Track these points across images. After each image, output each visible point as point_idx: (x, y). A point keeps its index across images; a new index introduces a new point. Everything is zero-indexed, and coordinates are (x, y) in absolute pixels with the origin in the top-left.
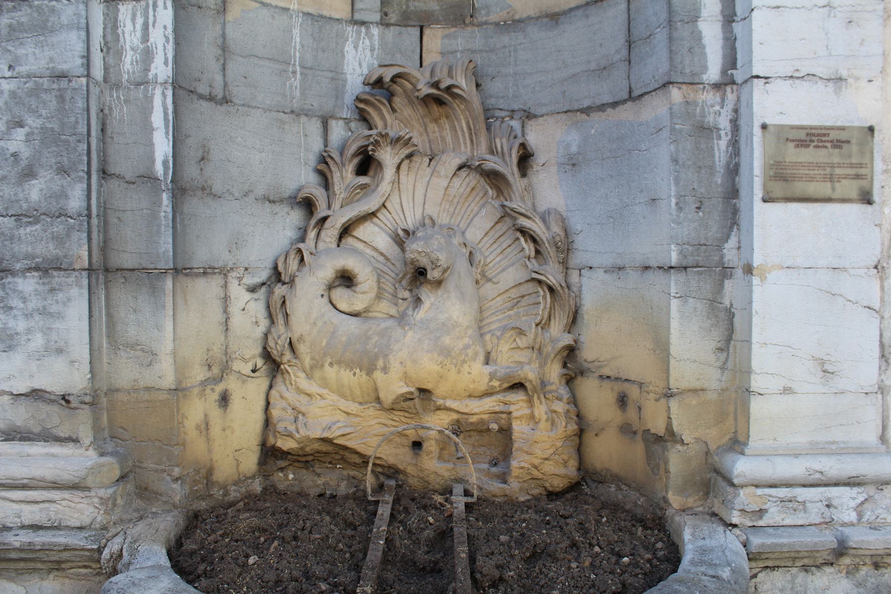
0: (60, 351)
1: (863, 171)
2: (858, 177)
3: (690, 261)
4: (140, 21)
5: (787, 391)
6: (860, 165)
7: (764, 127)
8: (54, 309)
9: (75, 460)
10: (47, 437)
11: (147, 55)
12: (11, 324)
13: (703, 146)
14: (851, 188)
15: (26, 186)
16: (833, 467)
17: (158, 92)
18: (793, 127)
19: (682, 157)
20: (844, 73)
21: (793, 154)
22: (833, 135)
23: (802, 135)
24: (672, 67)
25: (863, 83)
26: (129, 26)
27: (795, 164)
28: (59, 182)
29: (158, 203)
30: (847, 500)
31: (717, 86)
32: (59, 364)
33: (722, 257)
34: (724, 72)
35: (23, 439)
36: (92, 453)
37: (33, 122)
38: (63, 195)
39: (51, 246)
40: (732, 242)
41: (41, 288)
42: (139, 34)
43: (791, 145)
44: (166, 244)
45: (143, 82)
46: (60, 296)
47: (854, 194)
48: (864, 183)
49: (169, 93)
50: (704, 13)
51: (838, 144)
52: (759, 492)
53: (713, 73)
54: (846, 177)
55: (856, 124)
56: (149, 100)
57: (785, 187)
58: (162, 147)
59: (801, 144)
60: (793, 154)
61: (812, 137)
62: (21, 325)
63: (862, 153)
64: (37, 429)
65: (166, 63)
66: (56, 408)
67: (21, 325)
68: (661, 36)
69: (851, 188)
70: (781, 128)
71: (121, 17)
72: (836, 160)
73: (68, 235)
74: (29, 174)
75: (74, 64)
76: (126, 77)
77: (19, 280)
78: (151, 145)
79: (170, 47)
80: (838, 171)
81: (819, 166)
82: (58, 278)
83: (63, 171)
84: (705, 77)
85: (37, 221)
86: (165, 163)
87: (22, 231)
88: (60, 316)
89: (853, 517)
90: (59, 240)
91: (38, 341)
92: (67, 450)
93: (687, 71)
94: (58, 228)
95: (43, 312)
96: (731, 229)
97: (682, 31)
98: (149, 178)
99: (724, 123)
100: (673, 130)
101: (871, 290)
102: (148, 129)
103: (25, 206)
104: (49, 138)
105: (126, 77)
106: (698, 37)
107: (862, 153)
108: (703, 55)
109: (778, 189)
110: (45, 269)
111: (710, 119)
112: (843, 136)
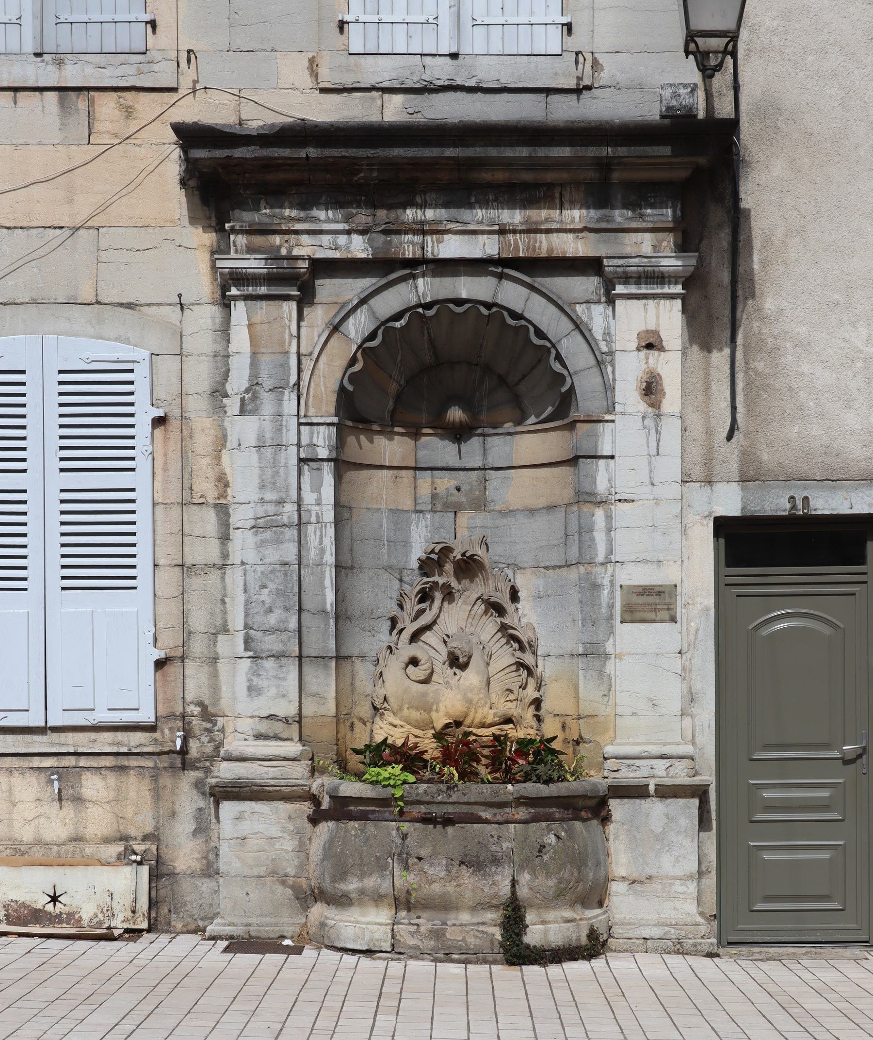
0: (284, 696)
1: (671, 607)
2: (668, 609)
3: (589, 651)
4: (318, 534)
5: (634, 714)
6: (669, 604)
7: (621, 586)
8: (281, 675)
9: (293, 748)
10: (277, 738)
11: (322, 551)
12: (260, 683)
13: (595, 594)
14: (665, 615)
15: (268, 616)
16: (655, 750)
17: (328, 569)
18: (635, 586)
19: (584, 600)
20: (661, 559)
21: (636, 599)
22: (656, 589)
23: (641, 590)
24: (580, 555)
25: (672, 563)
26: (313, 536)
27: (636, 604)
28: (285, 615)
29: (328, 624)
30: (661, 764)
31: (602, 564)
32: (283, 702)
33: (605, 649)
34: (606, 557)
35: (264, 739)
36: (298, 744)
37: (272, 586)
38: (287, 621)
39: (280, 645)
40: (611, 641)
41: (275, 665)
42: (318, 540)
43: (635, 595)
44: (332, 644)
45: (320, 564)
46: (284, 669)
47: (667, 617)
48: (672, 612)
49: (333, 570)
50: (596, 527)
51: (659, 594)
52: (617, 761)
53: (601, 558)
54: (663, 609)
55: (668, 583)
56: (323, 573)
57: (631, 614)
58: (330, 597)
59: (639, 594)
60: (636, 599)
61: (646, 591)
62: (265, 683)
63: (671, 597)
64: (271, 735)
65: (332, 555)
66: (281, 723)
67: (265, 683)
68: (576, 537)
69: (665, 615)
70: (629, 587)
71: (309, 532)
72: (658, 601)
73: (289, 640)
74: (270, 610)
75: (292, 557)
76: (311, 562)
77: (264, 661)
78: (324, 595)
79: (333, 547)
80: (658, 607)
81: (649, 604)
82: (284, 660)
83: (286, 609)
84: (596, 560)
85: (274, 633)
86: (331, 605)
87: (266, 638)
88: (283, 679)
89: (664, 773)
90: (284, 643)
91: (273, 691)
92: (288, 743)
93: (588, 557)
94: (284, 636)
95: (276, 677)
96: (610, 635)
97: (586, 537)
98: (324, 612)
99: (606, 582)
100: (580, 587)
101: (677, 664)
102: (323, 588)
103: (268, 626)
104: (280, 593)
105: (311, 562)
106: (593, 540)
107: (671, 597)
108: (596, 549)
109: (627, 617)
110: (279, 656)
111: (599, 581)
112: (661, 589)
